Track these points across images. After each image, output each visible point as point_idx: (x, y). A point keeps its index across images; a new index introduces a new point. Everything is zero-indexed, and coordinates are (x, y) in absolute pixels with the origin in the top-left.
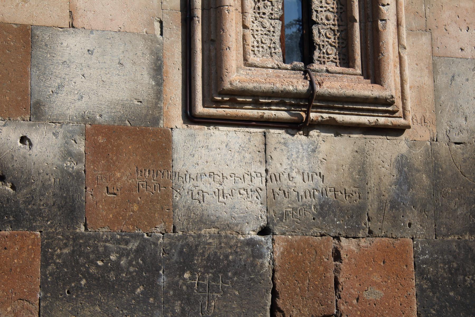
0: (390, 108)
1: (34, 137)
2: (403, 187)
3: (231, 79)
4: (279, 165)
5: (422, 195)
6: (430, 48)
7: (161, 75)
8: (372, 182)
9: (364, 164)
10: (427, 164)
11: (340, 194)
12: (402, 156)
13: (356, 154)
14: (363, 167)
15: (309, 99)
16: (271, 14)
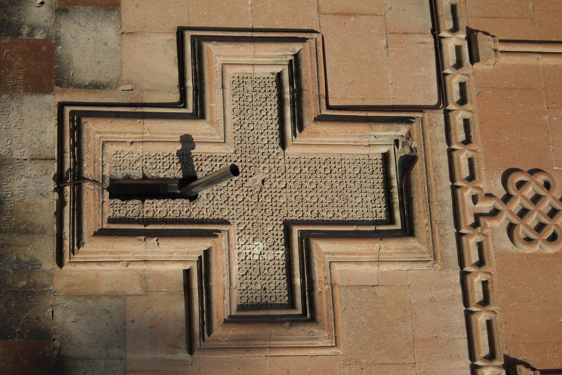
0: (76, 247)
1: (44, 9)
2: (15, 265)
3: (89, 122)
4: (29, 168)
5: (9, 281)
6: (131, 293)
7: (92, 89)
8: (18, 239)
9: (33, 234)
10: (35, 285)
11: (8, 213)
12: (41, 265)
13: (41, 227)
14: (30, 232)
15: (78, 178)
16: (146, 168)
